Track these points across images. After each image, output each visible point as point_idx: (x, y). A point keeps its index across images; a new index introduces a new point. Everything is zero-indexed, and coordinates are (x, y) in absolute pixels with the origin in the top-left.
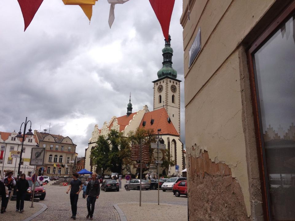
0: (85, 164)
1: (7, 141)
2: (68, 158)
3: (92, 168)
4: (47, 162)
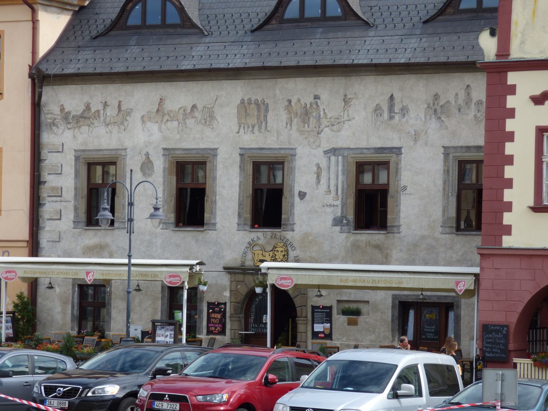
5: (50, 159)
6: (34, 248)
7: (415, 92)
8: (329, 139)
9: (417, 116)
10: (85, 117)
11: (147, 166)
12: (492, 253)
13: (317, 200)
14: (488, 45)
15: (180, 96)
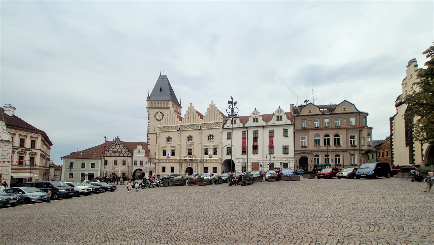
0: (392, 145)
1: (247, 125)
2: (353, 137)
3: (412, 151)
4: (312, 147)
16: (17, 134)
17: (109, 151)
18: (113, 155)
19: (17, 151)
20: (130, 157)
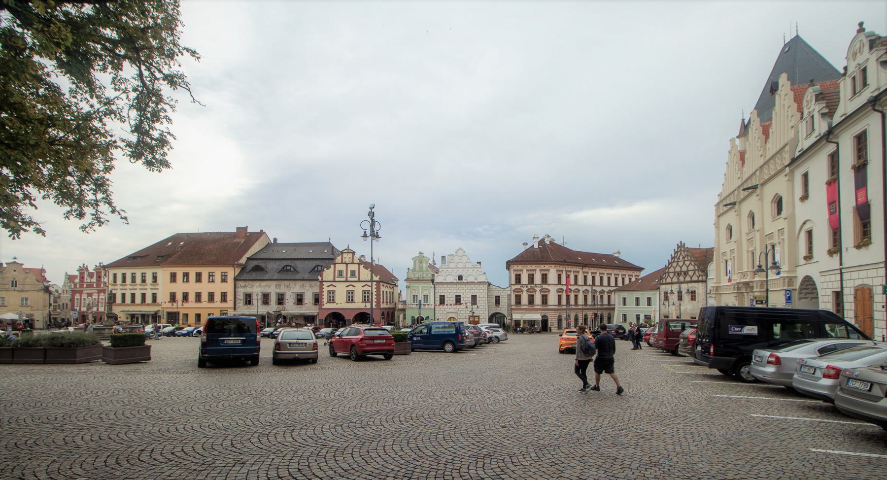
5: (238, 294)
6: (235, 309)
7: (307, 284)
8: (292, 290)
9: (308, 287)
10: (245, 286)
11: (257, 295)
12: (320, 309)
13: (290, 300)
14: (320, 278)
15: (264, 283)
16: (525, 270)
17: (669, 273)
18: (675, 280)
19: (525, 289)
20: (702, 281)
